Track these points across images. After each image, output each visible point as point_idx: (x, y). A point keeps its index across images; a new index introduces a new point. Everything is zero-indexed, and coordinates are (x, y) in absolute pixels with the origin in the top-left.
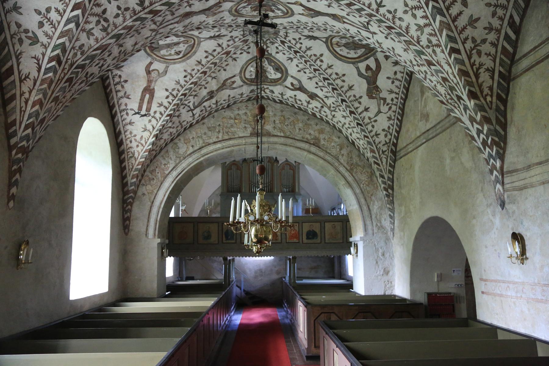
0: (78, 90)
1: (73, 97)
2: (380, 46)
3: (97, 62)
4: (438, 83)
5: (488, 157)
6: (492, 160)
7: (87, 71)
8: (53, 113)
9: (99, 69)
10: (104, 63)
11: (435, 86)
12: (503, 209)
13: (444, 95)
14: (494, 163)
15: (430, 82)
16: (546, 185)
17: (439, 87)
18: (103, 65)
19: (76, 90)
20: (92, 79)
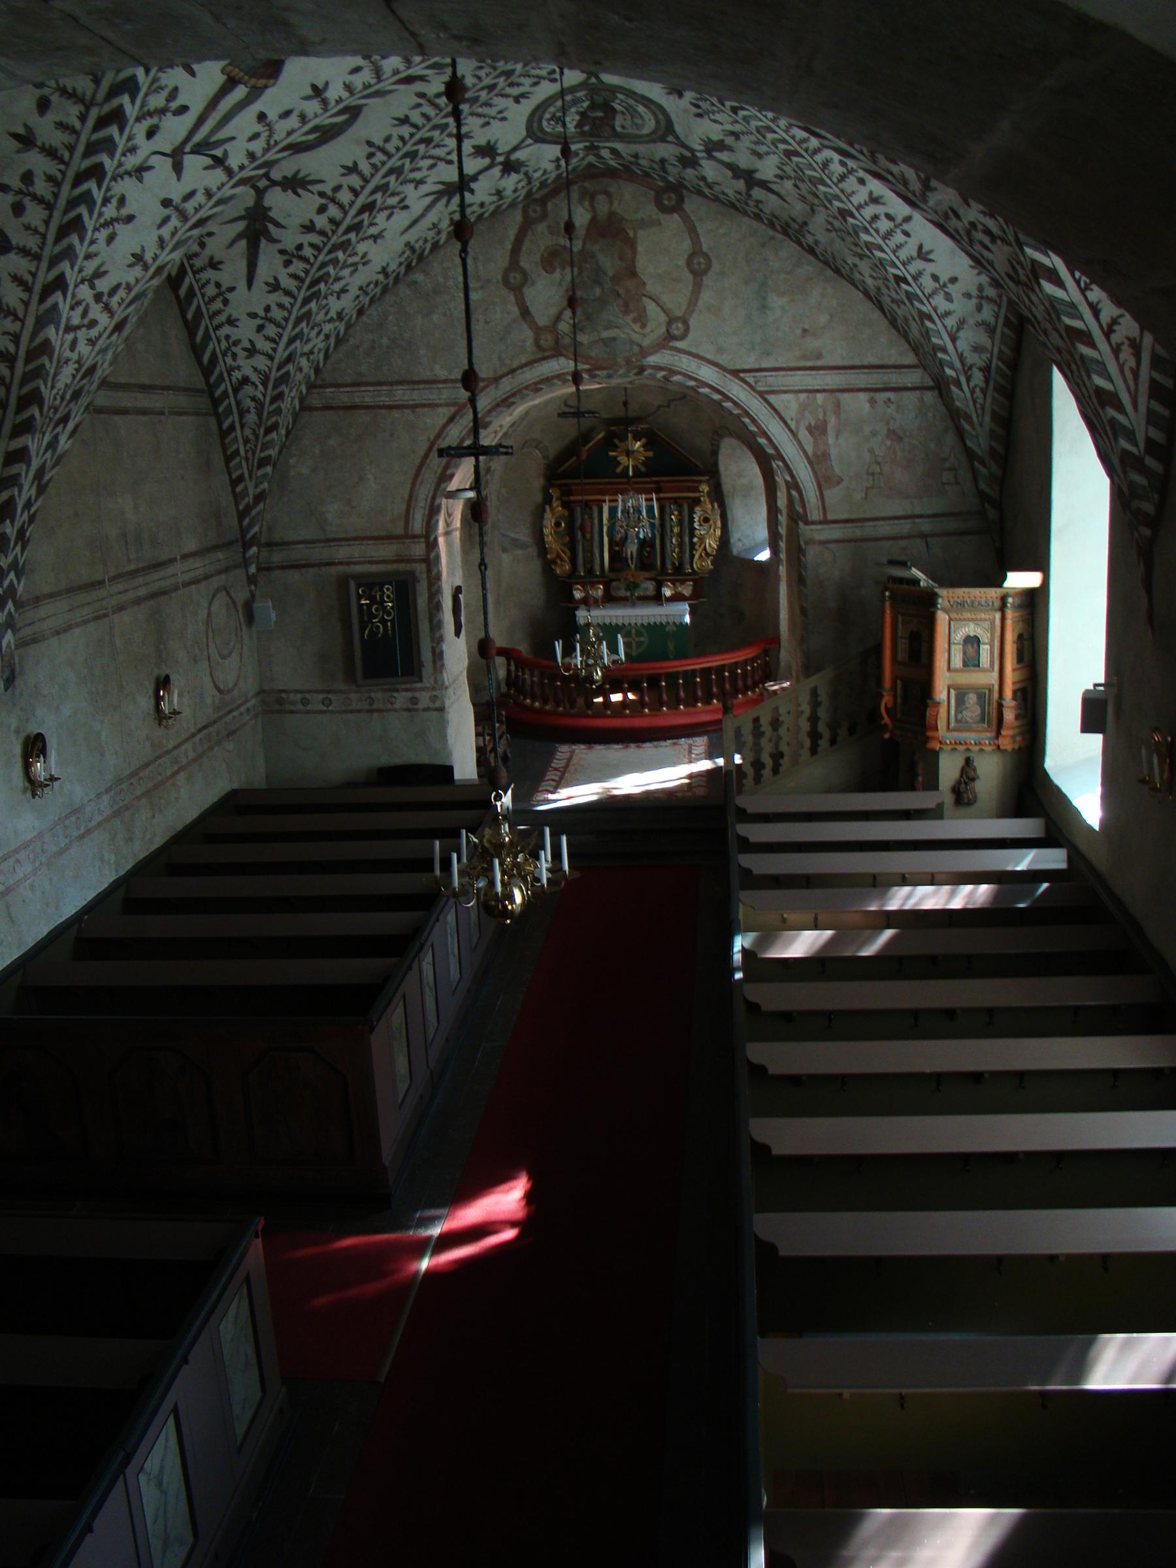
0: (1049, 314)
1: (1064, 334)
2: (129, 173)
3: (978, 247)
4: (78, 362)
5: (9, 566)
6: (12, 575)
7: (1003, 275)
8: (1083, 394)
9: (999, 242)
10: (980, 227)
11: (67, 361)
12: (6, 690)
13: (54, 391)
14: (15, 582)
15: (67, 345)
16: (62, 636)
17: (69, 370)
18: (987, 232)
19: (1048, 318)
20: (1023, 268)
